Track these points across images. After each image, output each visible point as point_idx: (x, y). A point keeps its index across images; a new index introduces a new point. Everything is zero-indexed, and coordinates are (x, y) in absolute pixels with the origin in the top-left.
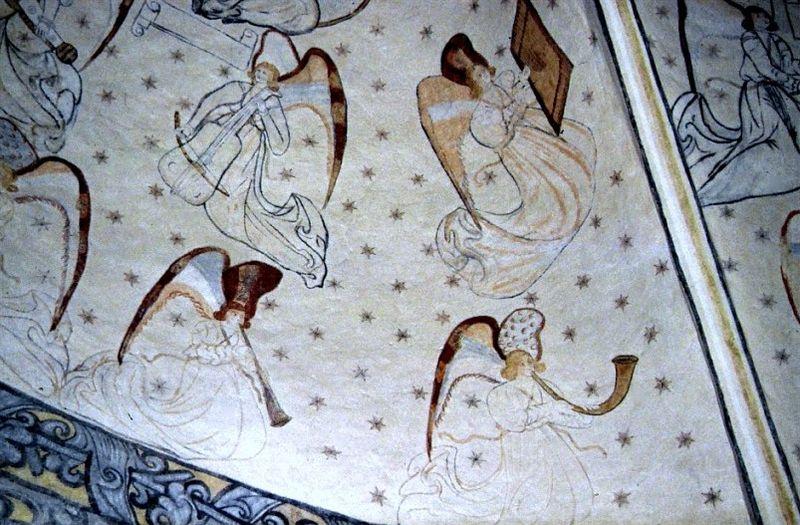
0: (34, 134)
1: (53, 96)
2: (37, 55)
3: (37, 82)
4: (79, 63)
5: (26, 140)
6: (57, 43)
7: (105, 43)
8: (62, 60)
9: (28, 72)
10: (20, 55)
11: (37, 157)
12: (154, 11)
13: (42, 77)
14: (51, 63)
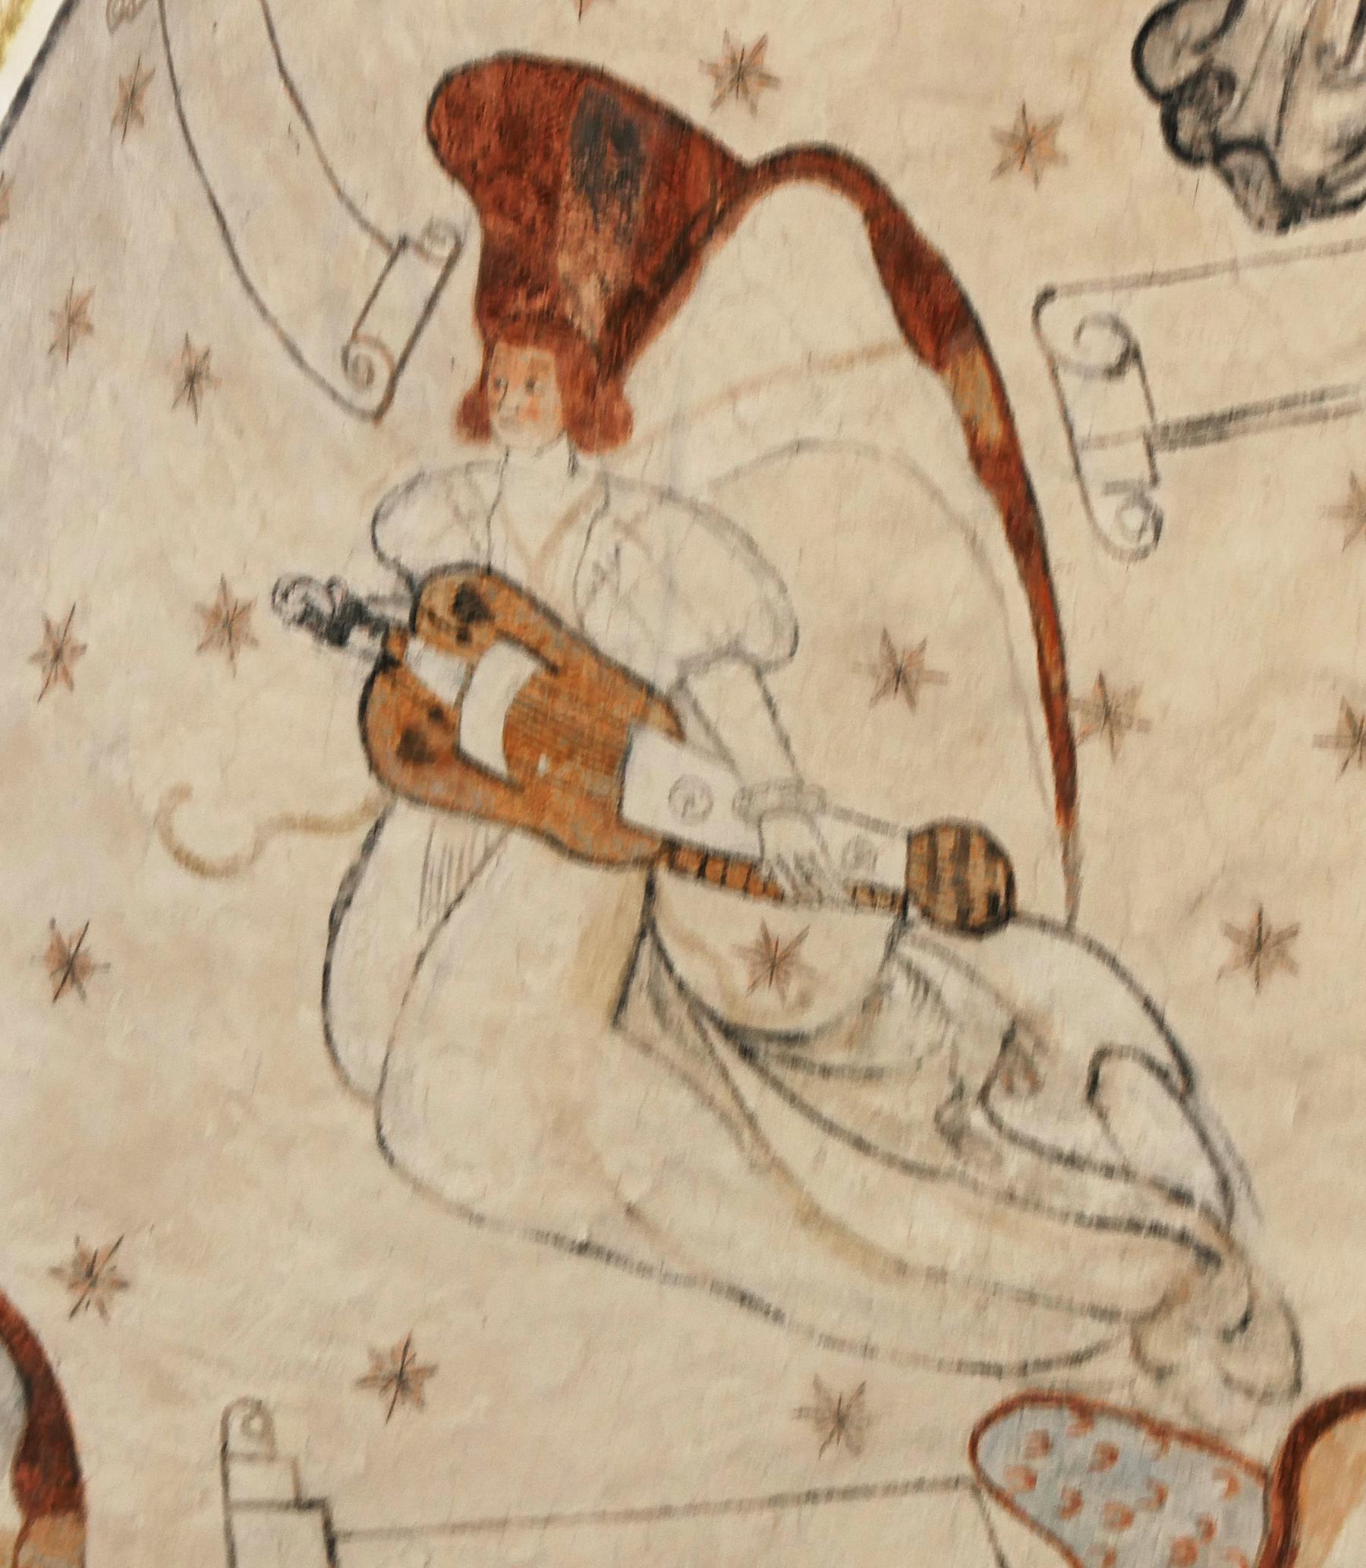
0: (1162, 1374)
1: (1081, 1134)
2: (874, 999)
3: (977, 1119)
4: (1039, 889)
5: (1161, 1432)
6: (892, 868)
7: (1054, 698)
8: (970, 927)
9: (913, 1104)
10: (837, 1057)
11: (1262, 1474)
12: (1115, 371)
13: (975, 1082)
14: (953, 987)
